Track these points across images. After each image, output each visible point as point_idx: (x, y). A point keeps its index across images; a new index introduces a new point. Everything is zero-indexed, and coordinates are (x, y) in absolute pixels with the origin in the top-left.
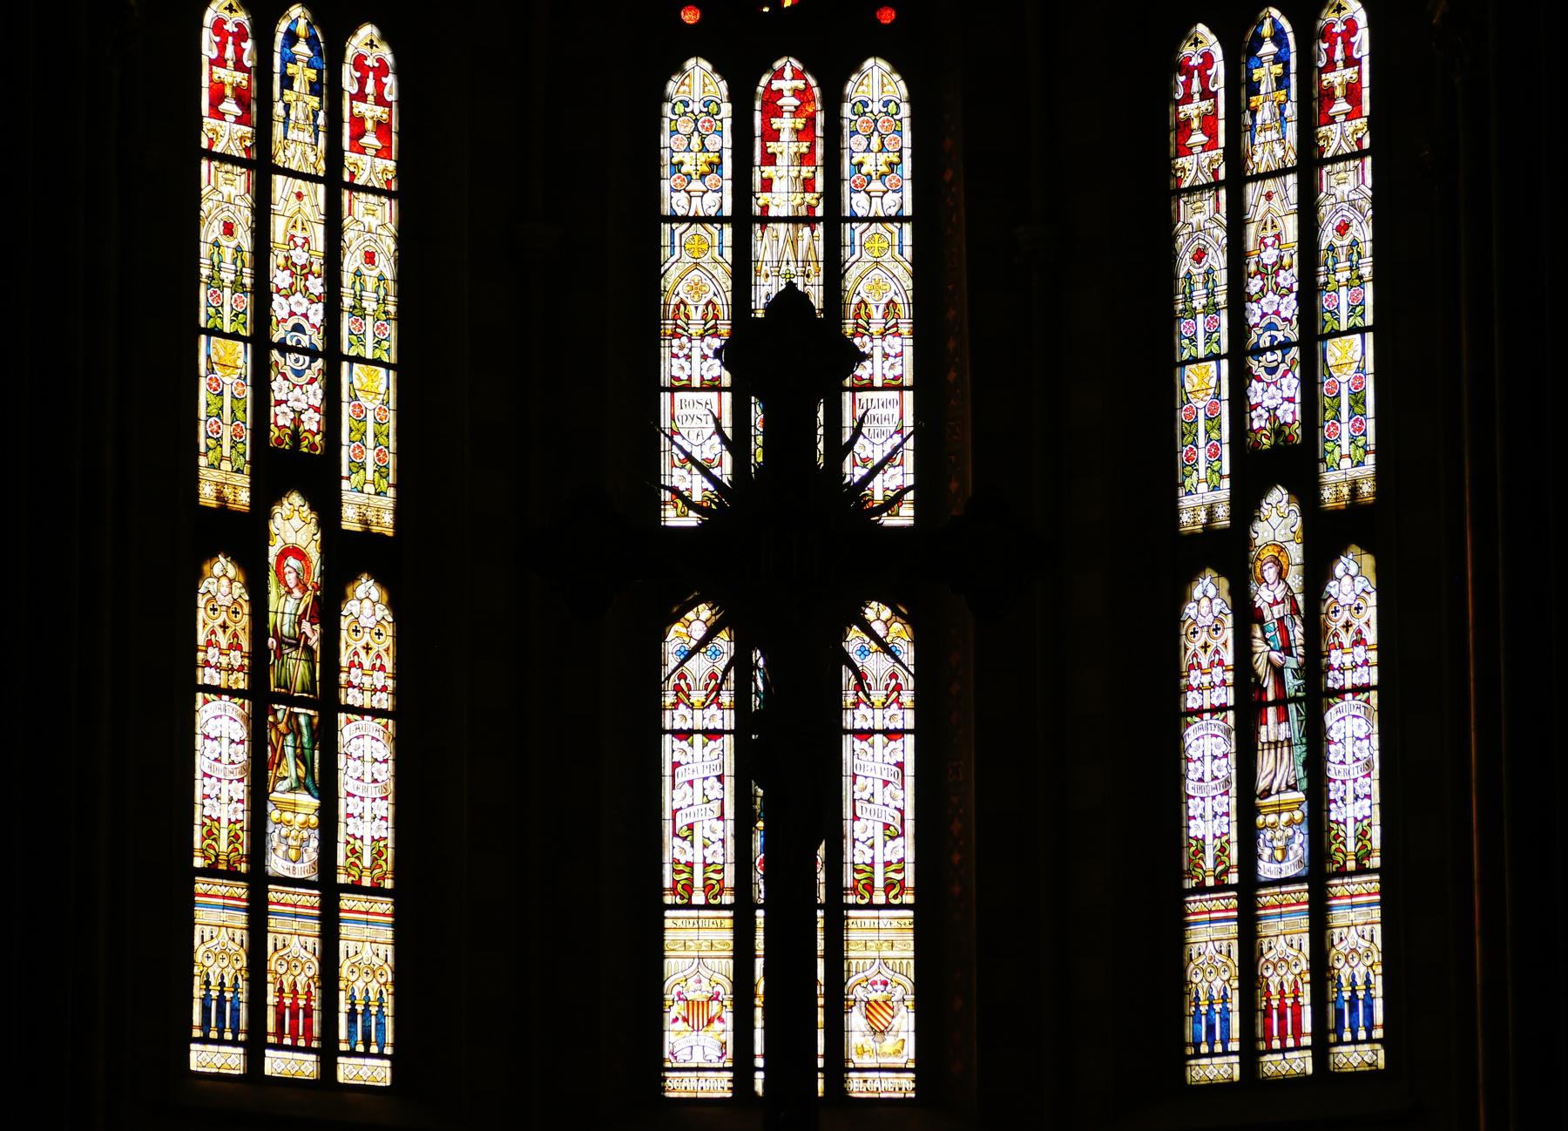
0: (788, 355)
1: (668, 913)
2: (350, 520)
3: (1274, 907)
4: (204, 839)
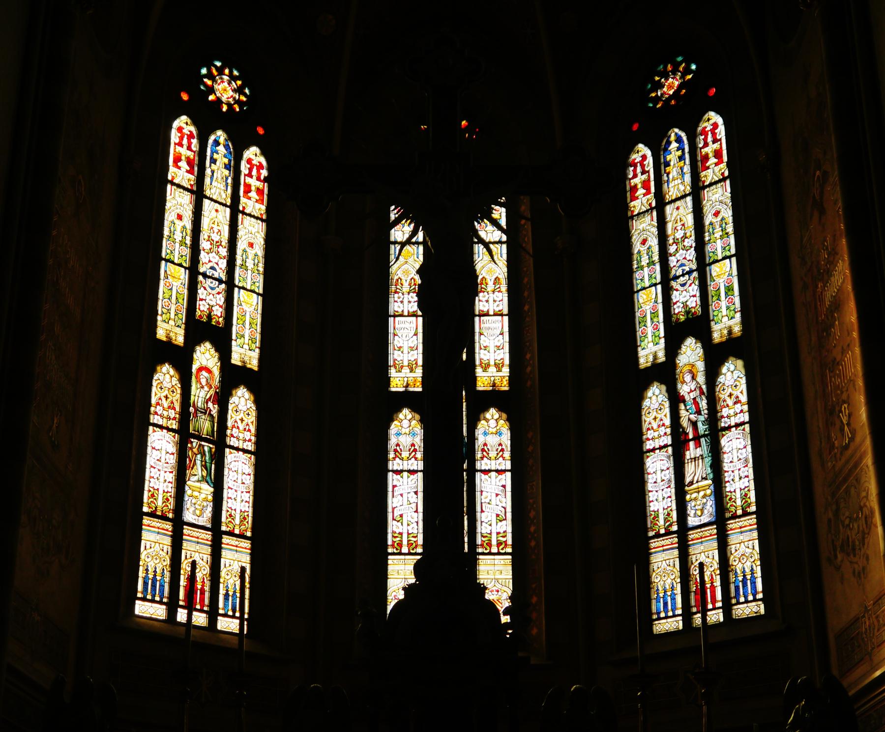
1: (390, 557)
2: (236, 360)
3: (698, 539)
4: (149, 498)
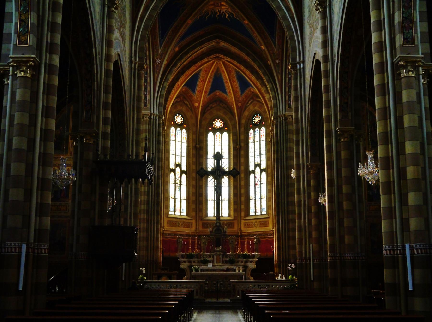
0: (218, 157)
